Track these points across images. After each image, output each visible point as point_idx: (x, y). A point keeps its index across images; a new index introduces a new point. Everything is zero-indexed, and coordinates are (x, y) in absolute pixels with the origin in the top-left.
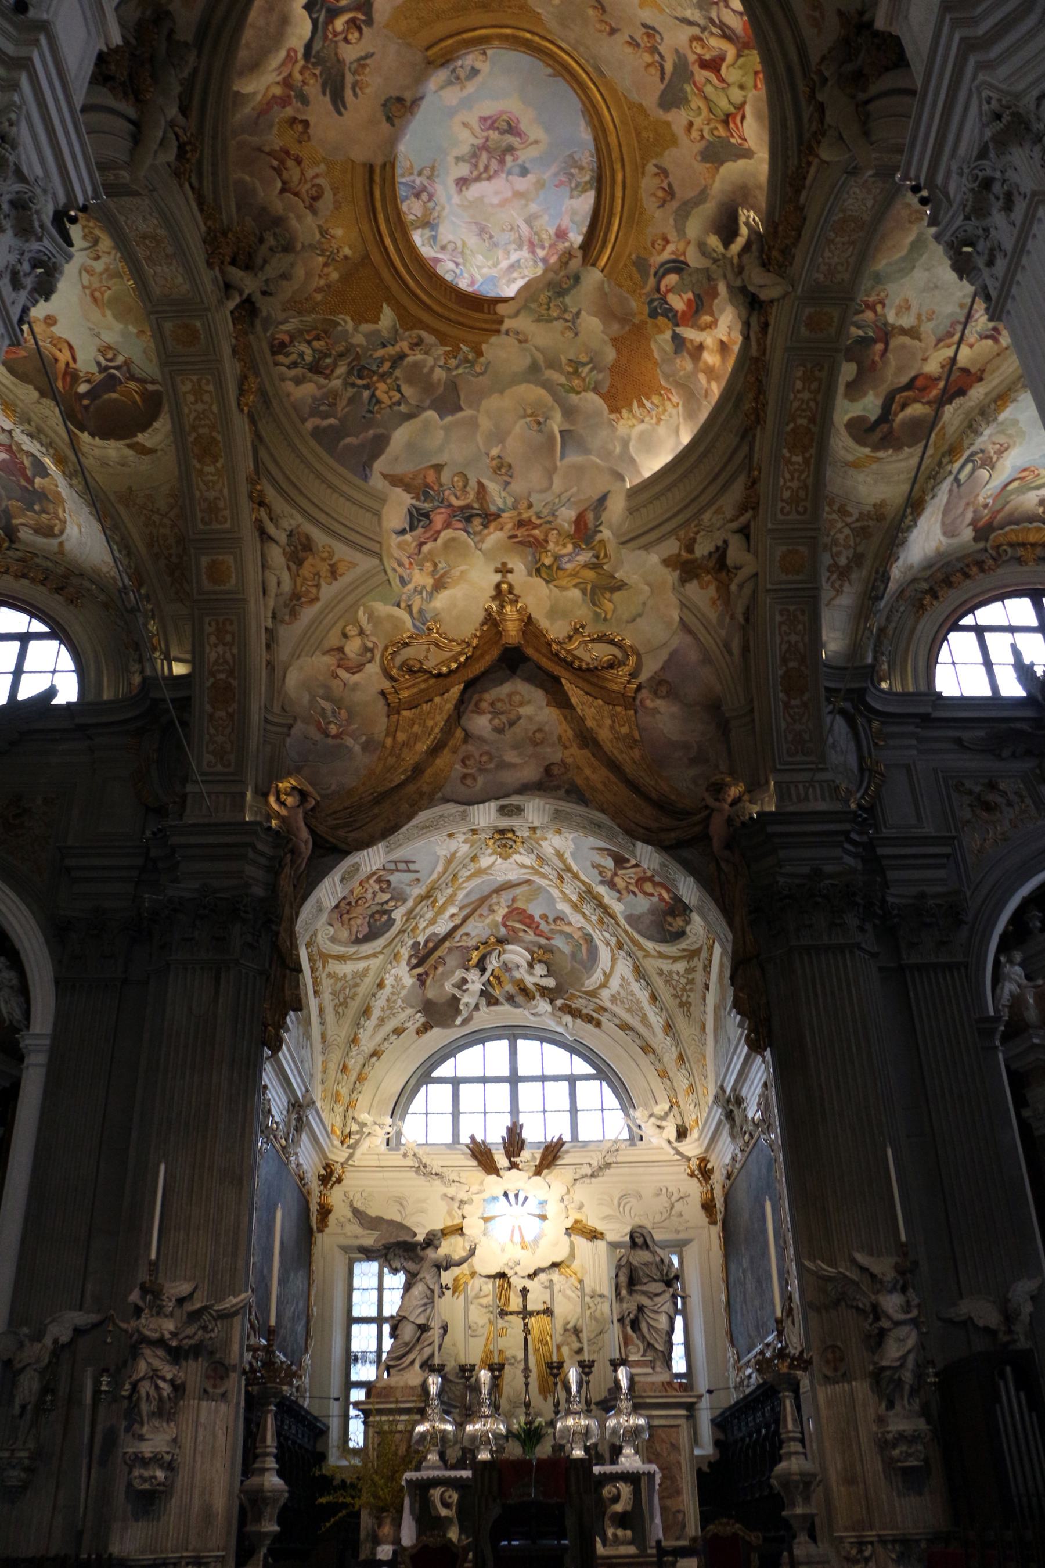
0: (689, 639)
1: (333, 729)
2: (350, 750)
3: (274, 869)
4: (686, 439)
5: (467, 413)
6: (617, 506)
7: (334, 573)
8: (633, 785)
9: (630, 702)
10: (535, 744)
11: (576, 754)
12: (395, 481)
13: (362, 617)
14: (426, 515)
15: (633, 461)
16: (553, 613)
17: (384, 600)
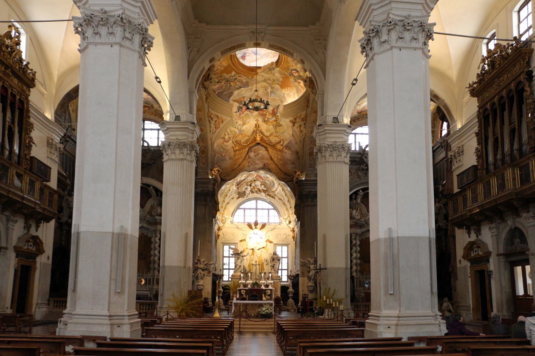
0: (293, 138)
1: (223, 155)
2: (227, 160)
3: (214, 185)
4: (297, 98)
5: (250, 87)
6: (281, 109)
7: (222, 122)
8: (280, 169)
9: (281, 151)
10: (262, 159)
11: (270, 162)
12: (235, 101)
13: (229, 131)
14: (241, 108)
15: (285, 98)
16: (267, 131)
17: (233, 126)
